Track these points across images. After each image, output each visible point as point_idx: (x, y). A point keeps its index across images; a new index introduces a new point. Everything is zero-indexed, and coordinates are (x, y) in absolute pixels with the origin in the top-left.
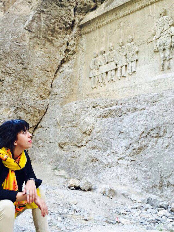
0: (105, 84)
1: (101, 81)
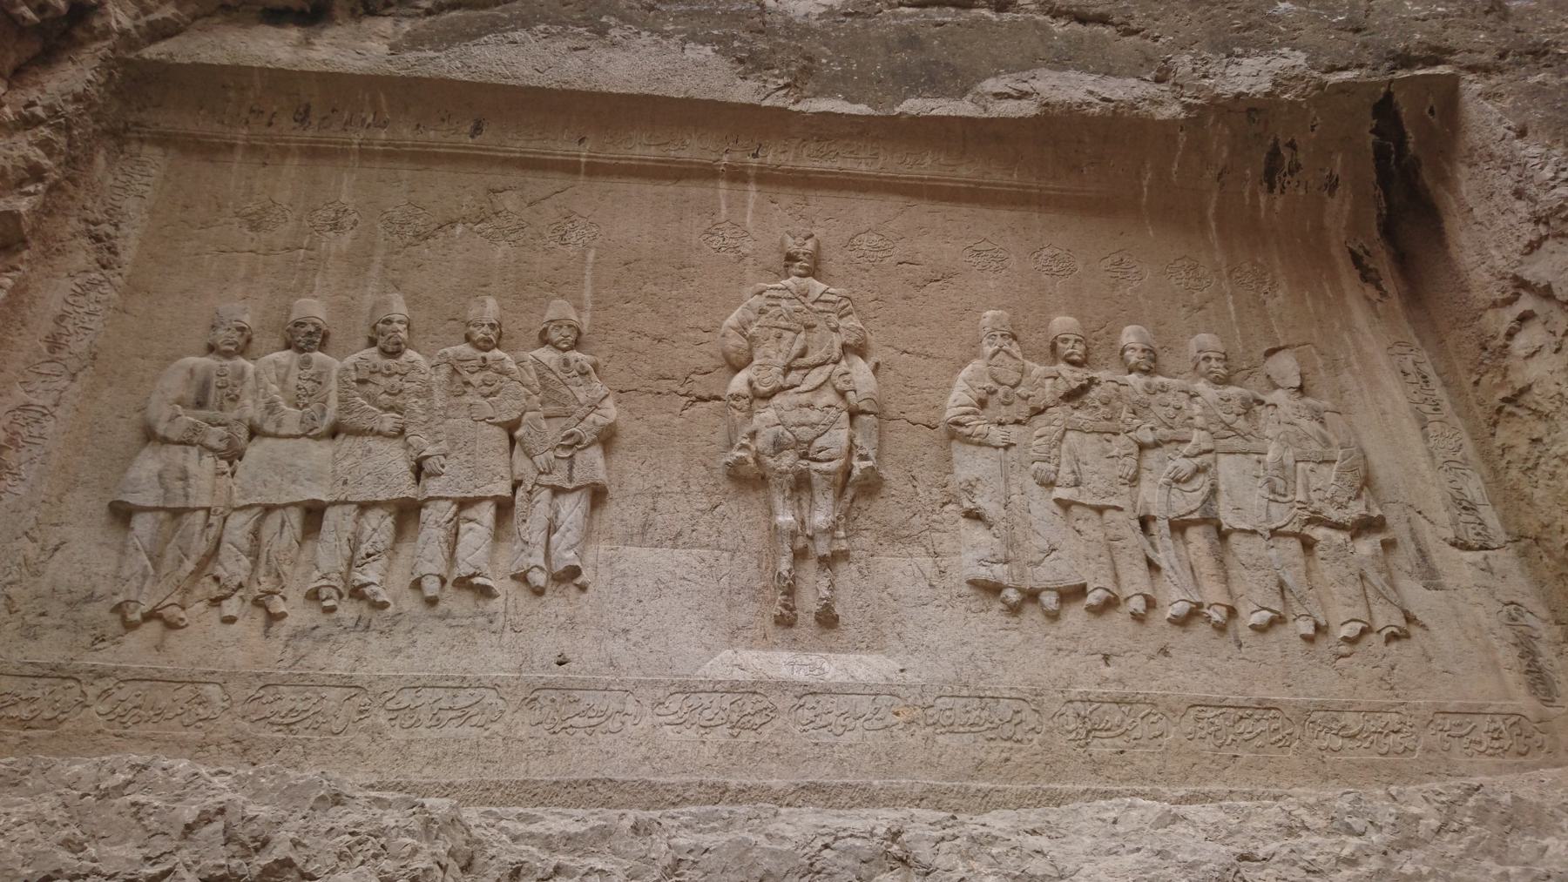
0: (278, 605)
1: (233, 566)
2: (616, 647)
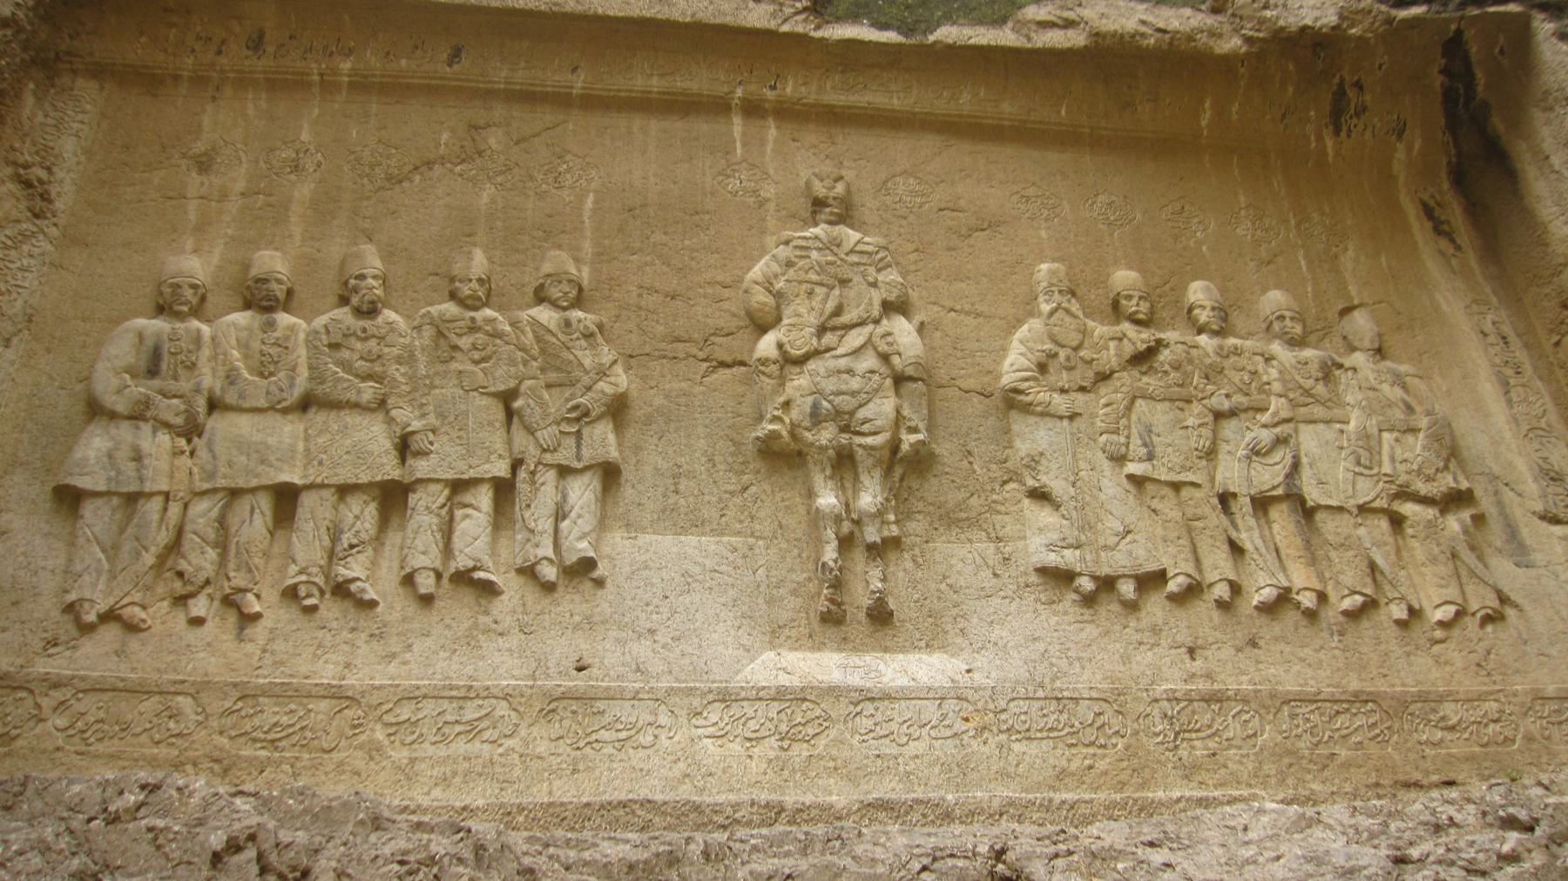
1: (200, 560)
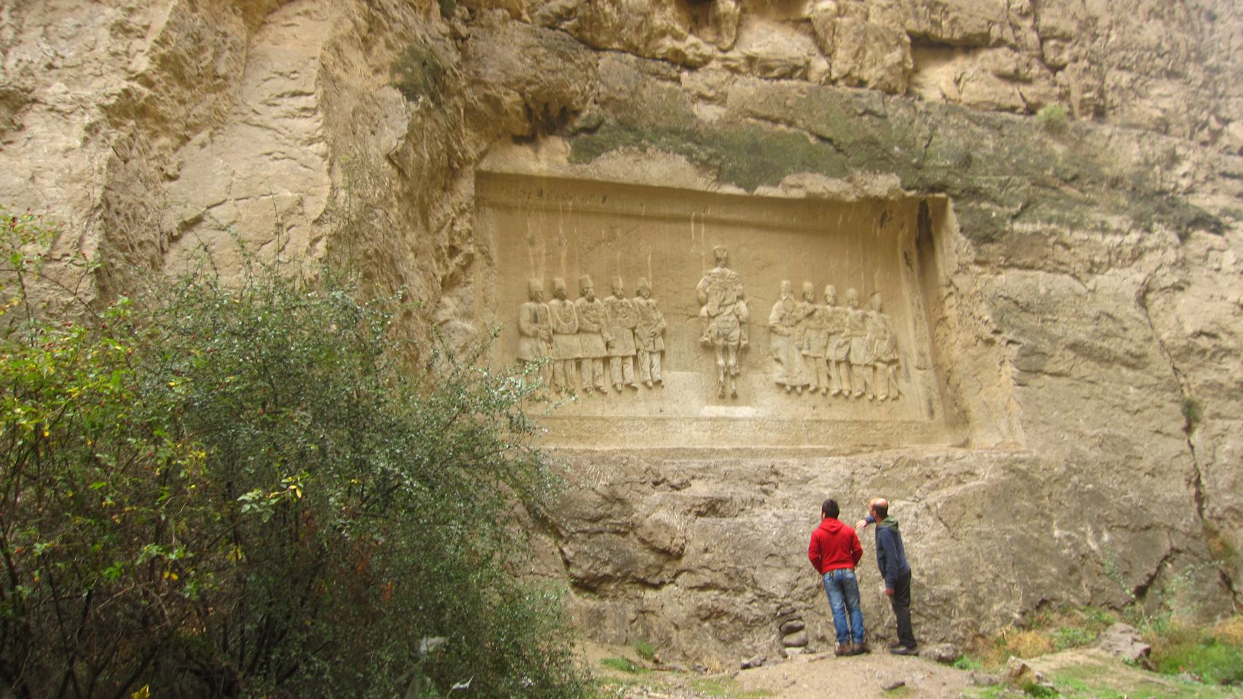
2: (675, 406)
